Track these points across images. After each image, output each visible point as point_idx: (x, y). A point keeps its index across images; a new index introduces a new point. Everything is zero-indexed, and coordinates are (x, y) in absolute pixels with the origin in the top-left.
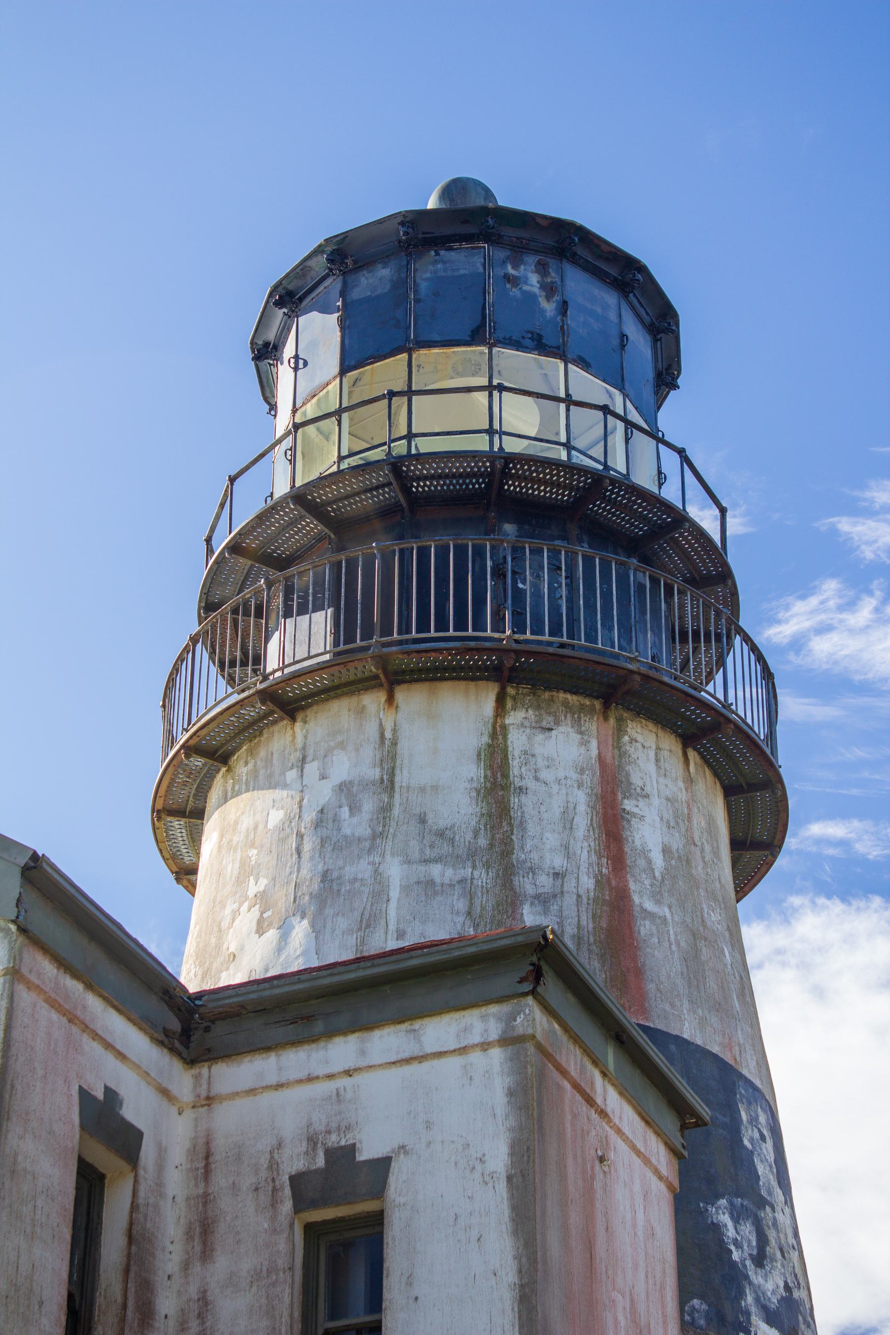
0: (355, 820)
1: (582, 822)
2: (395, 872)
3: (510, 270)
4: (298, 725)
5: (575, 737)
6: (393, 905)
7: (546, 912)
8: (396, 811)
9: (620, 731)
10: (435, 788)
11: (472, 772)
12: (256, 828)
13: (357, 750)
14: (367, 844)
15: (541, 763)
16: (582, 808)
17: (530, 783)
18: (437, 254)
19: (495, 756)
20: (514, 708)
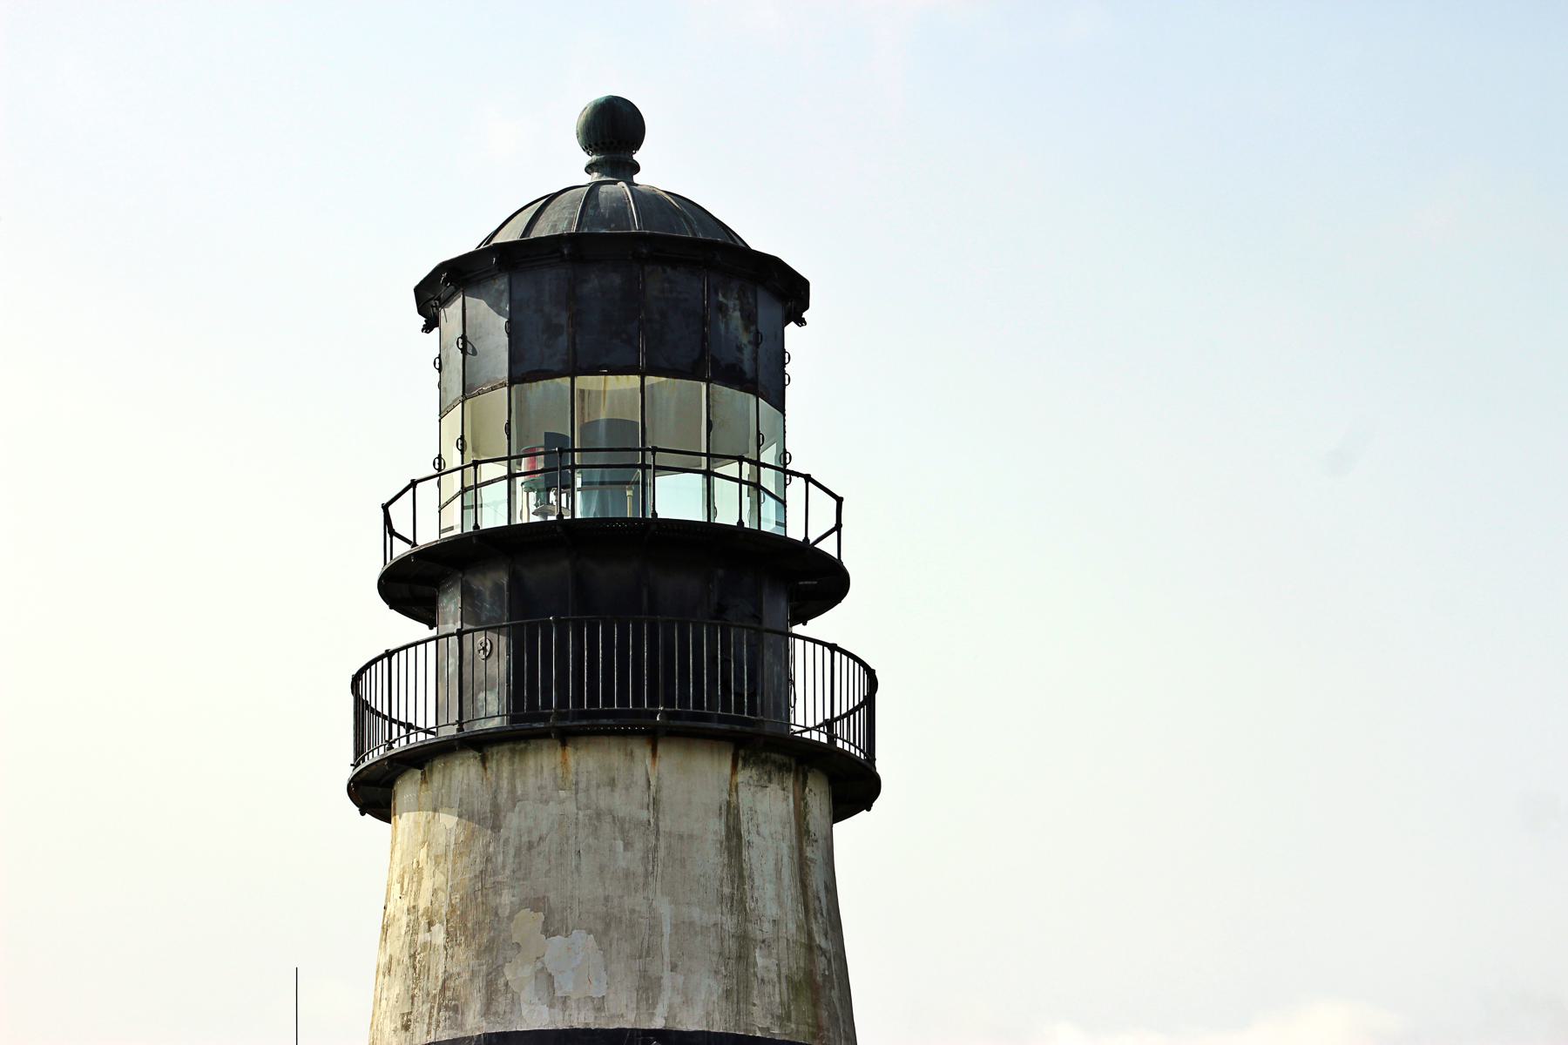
0: (629, 854)
1: (786, 874)
2: (665, 909)
3: (721, 298)
4: (569, 750)
5: (781, 793)
6: (666, 939)
7: (770, 955)
8: (662, 853)
9: (805, 784)
10: (691, 836)
11: (717, 826)
12: (530, 832)
13: (627, 789)
14: (641, 880)
15: (761, 819)
16: (786, 859)
17: (754, 838)
18: (664, 271)
19: (731, 813)
20: (744, 766)
